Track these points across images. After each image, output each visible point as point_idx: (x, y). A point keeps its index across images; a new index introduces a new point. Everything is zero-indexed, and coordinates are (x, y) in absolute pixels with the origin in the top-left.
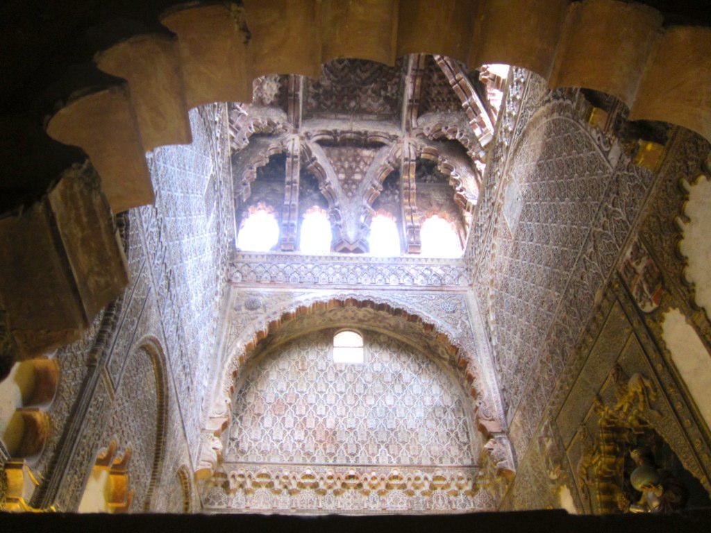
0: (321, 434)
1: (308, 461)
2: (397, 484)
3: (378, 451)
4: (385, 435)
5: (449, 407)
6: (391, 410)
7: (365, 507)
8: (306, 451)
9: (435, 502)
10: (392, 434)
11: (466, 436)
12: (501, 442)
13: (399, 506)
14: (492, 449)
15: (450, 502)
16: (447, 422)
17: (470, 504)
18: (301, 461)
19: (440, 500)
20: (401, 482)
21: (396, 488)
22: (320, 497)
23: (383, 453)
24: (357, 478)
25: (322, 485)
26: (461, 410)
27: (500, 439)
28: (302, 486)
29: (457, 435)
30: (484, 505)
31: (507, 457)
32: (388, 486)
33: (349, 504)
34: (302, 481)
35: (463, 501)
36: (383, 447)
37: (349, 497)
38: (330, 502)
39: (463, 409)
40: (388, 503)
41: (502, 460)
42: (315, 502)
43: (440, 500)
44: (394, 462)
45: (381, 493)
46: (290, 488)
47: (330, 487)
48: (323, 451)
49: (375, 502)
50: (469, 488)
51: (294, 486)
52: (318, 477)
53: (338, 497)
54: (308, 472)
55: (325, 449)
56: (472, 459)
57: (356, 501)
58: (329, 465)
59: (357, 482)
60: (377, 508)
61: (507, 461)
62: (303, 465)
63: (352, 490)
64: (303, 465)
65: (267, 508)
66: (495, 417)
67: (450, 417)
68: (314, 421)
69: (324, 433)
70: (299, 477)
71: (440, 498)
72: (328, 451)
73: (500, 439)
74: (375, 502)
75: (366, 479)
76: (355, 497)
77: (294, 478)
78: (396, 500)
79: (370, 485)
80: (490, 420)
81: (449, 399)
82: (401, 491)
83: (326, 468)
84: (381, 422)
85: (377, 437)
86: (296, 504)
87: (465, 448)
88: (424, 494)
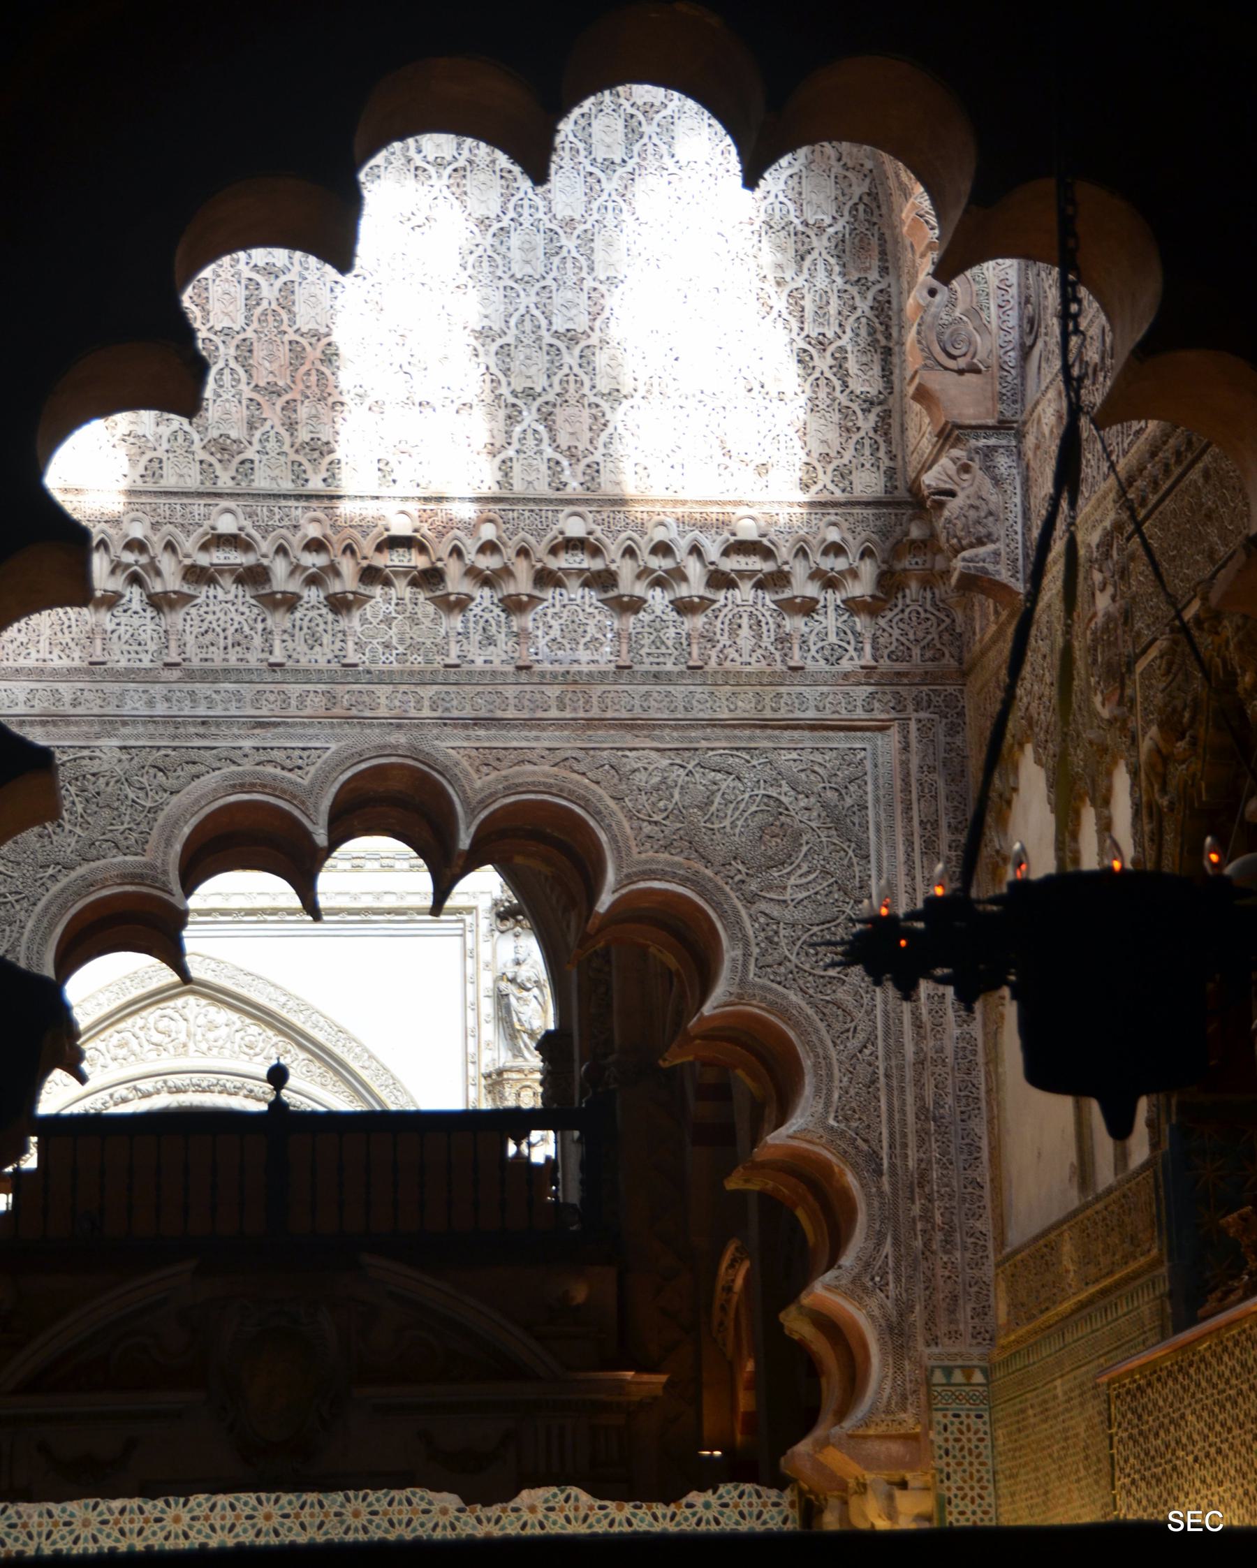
0: (271, 357)
1: (225, 482)
2: (582, 571)
3: (508, 433)
4: (542, 360)
5: (822, 230)
6: (569, 243)
7: (453, 660)
8: (214, 433)
9: (724, 640)
10: (570, 359)
11: (877, 370)
12: (989, 469)
13: (584, 655)
14: (952, 494)
15: (783, 640)
16: (808, 304)
17: (859, 650)
18: (193, 480)
19: (745, 631)
20: (597, 564)
21: (573, 583)
22: (279, 621)
23: (531, 442)
24: (423, 549)
25: (281, 578)
26: (875, 241)
27: (989, 453)
28: (198, 575)
29: (840, 366)
30: (916, 652)
31: (999, 530)
32: (545, 578)
33: (387, 646)
34: (203, 559)
35: (833, 638)
36: (529, 417)
37: (388, 621)
38: (314, 640)
39: (882, 237)
40: (542, 643)
41: (980, 542)
42: (258, 641)
43: (745, 631)
44: (574, 487)
45: (513, 606)
46: (157, 586)
47: (313, 580)
48: (285, 435)
49: (490, 641)
50: (861, 588)
51: (171, 580)
52: (266, 546)
53: (344, 623)
54: (227, 525)
55: (291, 426)
56: (891, 473)
57: (413, 632)
58: (309, 497)
59: (419, 561)
60: (497, 662)
61: (1000, 546)
62: (200, 495)
63: (402, 589)
64: (200, 495)
65: (66, 663)
66: (982, 354)
67: (821, 280)
68: (241, 293)
69: (284, 353)
70: (189, 544)
71: (745, 621)
72: (303, 435)
73: (989, 453)
74: (490, 641)
75: (457, 552)
76: (414, 620)
77: (170, 547)
78: (573, 632)
79: (472, 573)
80: (961, 372)
81: (831, 190)
82: (592, 596)
83: (297, 510)
84: (527, 299)
85: (506, 372)
86: (182, 646)
87: (867, 423)
88: (684, 607)
